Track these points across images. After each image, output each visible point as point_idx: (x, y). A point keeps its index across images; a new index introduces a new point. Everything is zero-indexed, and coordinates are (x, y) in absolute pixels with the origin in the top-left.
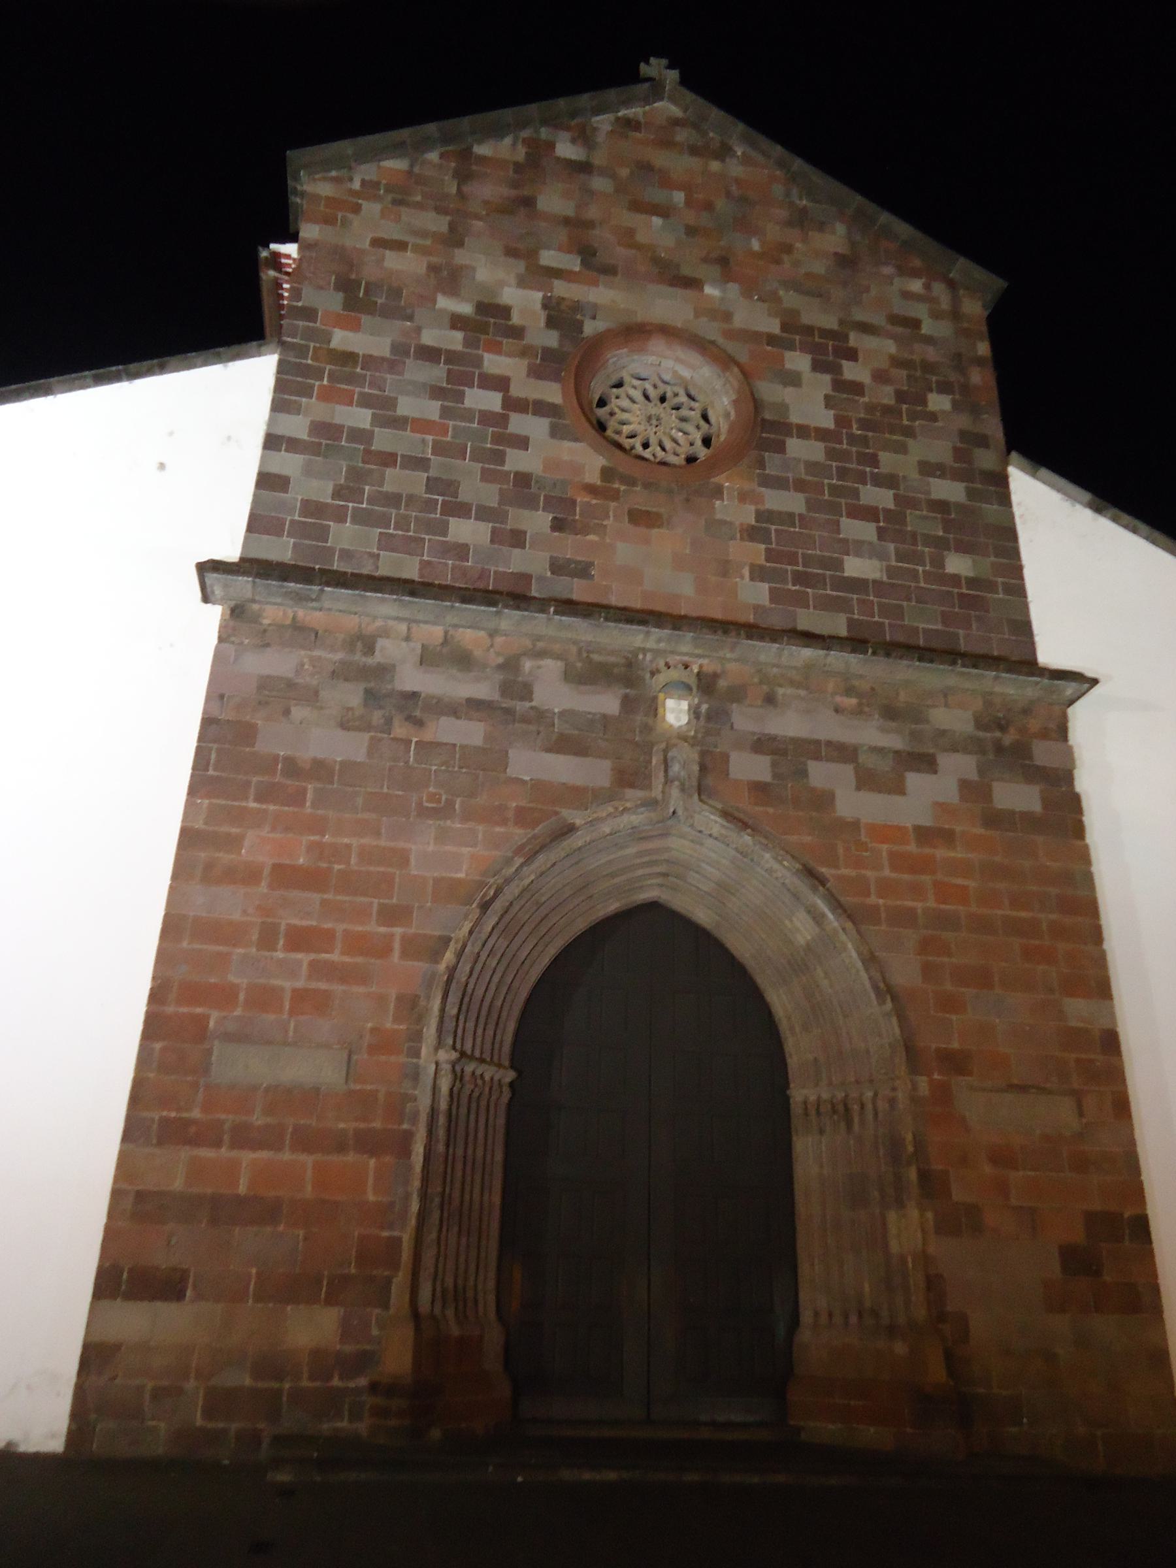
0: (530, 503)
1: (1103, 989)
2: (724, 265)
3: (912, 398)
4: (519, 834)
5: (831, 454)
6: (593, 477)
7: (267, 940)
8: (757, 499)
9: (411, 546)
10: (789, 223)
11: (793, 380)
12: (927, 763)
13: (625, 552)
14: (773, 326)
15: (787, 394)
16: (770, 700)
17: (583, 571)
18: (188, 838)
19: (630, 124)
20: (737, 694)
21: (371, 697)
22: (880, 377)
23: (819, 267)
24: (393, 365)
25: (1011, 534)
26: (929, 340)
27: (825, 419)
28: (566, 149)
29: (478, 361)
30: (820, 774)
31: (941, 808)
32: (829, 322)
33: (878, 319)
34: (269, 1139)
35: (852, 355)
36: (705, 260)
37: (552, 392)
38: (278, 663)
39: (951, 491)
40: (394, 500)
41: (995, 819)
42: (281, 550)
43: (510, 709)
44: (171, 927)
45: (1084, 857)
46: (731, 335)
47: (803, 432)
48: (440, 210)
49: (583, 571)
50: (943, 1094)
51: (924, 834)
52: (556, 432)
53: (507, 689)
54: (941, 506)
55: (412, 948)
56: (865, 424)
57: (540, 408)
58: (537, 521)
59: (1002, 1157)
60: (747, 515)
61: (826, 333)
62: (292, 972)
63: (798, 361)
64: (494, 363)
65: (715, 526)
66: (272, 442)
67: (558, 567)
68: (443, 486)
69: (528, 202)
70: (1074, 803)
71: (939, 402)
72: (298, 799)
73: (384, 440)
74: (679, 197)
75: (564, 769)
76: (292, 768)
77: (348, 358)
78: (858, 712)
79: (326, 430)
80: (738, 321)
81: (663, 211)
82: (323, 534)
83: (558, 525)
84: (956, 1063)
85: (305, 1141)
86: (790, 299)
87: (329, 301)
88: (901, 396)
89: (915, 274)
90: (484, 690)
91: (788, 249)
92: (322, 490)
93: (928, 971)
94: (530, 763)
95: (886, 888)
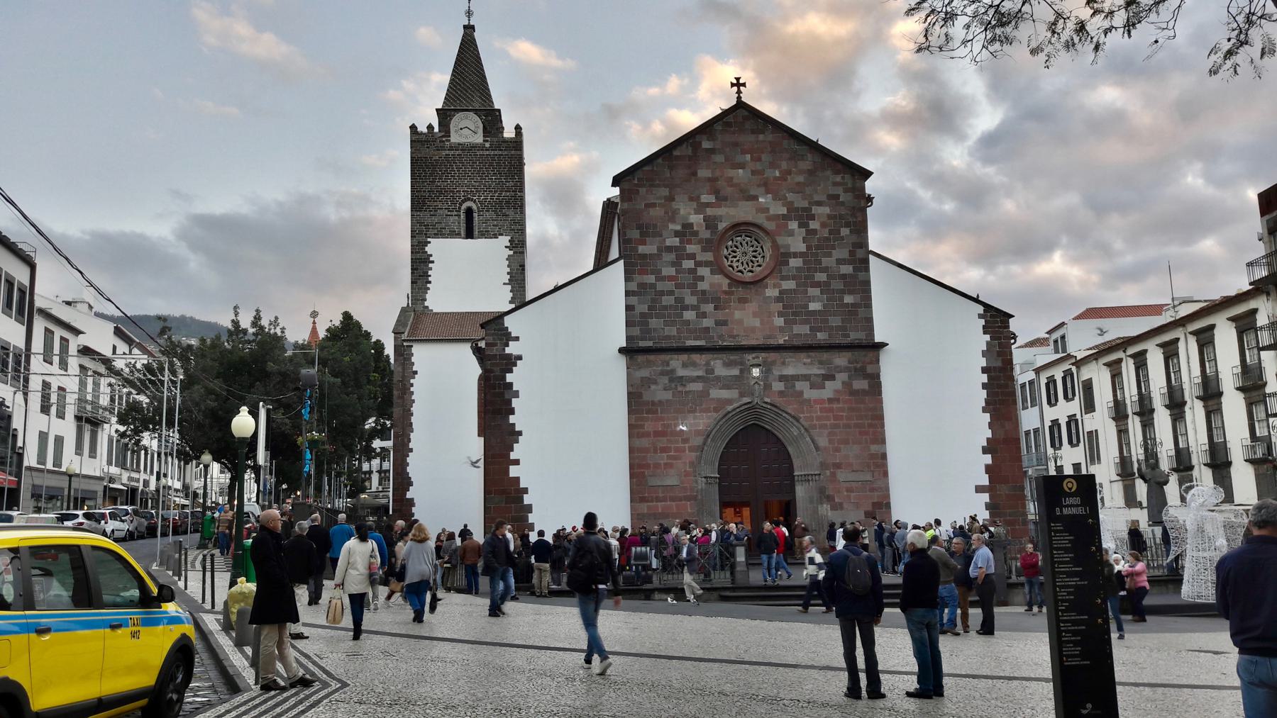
0: (706, 301)
1: (883, 441)
2: (767, 187)
3: (835, 232)
4: (715, 415)
5: (804, 263)
6: (725, 288)
7: (655, 451)
8: (780, 286)
9: (673, 323)
10: (790, 159)
11: (791, 233)
12: (832, 378)
13: (737, 315)
14: (784, 211)
15: (789, 240)
16: (784, 363)
17: (724, 323)
18: (630, 426)
19: (728, 124)
20: (773, 363)
21: (671, 380)
22: (823, 225)
23: (801, 179)
24: (659, 256)
25: (867, 283)
26: (843, 203)
27: (802, 248)
28: (706, 145)
29: (685, 249)
30: (799, 385)
31: (836, 391)
32: (805, 204)
33: (823, 198)
34: (664, 500)
35: (812, 218)
36: (759, 186)
37: (709, 256)
38: (644, 373)
39: (847, 269)
40: (665, 308)
41: (854, 393)
42: (636, 331)
43: (709, 379)
44: (632, 450)
45: (881, 402)
46: (769, 219)
47: (795, 255)
48: (666, 186)
49: (724, 323)
50: (833, 474)
51: (830, 400)
52: (712, 272)
53: (707, 372)
54: (844, 277)
55: (692, 449)
56: (818, 247)
57: (707, 264)
58: (709, 308)
59: (849, 490)
60: (776, 293)
61: (804, 209)
62: (663, 458)
63: (793, 225)
64: (691, 248)
65: (767, 300)
66: (628, 293)
67: (718, 323)
68: (680, 300)
69: (695, 174)
70: (879, 385)
71: (845, 231)
72: (656, 412)
73: (660, 286)
74: (748, 157)
75: (725, 394)
76: (653, 403)
77: (644, 256)
78: (811, 364)
79: (642, 286)
80: (772, 212)
81: (742, 166)
82: (647, 324)
83: (716, 308)
84: (838, 466)
85: (672, 499)
86: (790, 197)
87: (634, 234)
88: (831, 232)
89: (837, 173)
90: (700, 373)
91: (789, 172)
92: (644, 308)
93: (830, 441)
94: (716, 393)
95: (819, 418)
